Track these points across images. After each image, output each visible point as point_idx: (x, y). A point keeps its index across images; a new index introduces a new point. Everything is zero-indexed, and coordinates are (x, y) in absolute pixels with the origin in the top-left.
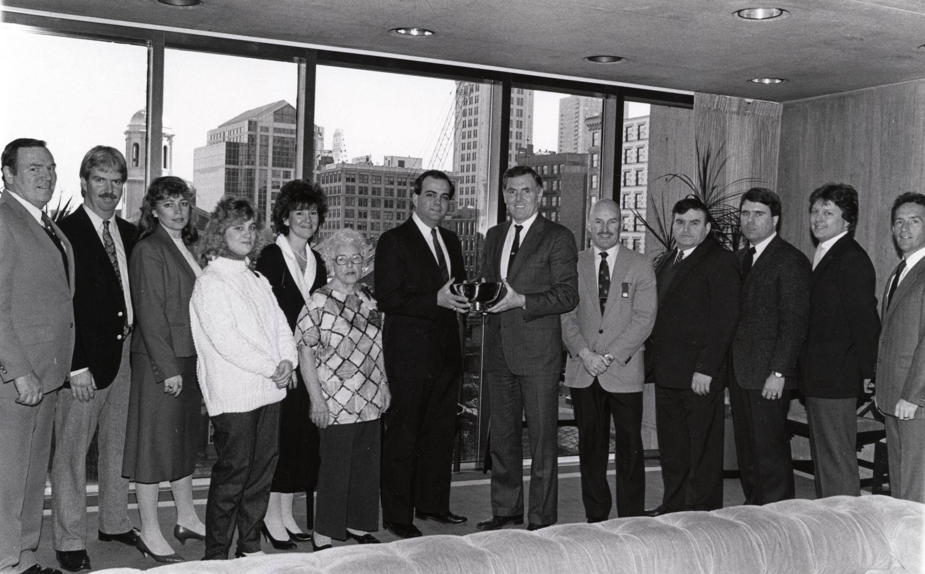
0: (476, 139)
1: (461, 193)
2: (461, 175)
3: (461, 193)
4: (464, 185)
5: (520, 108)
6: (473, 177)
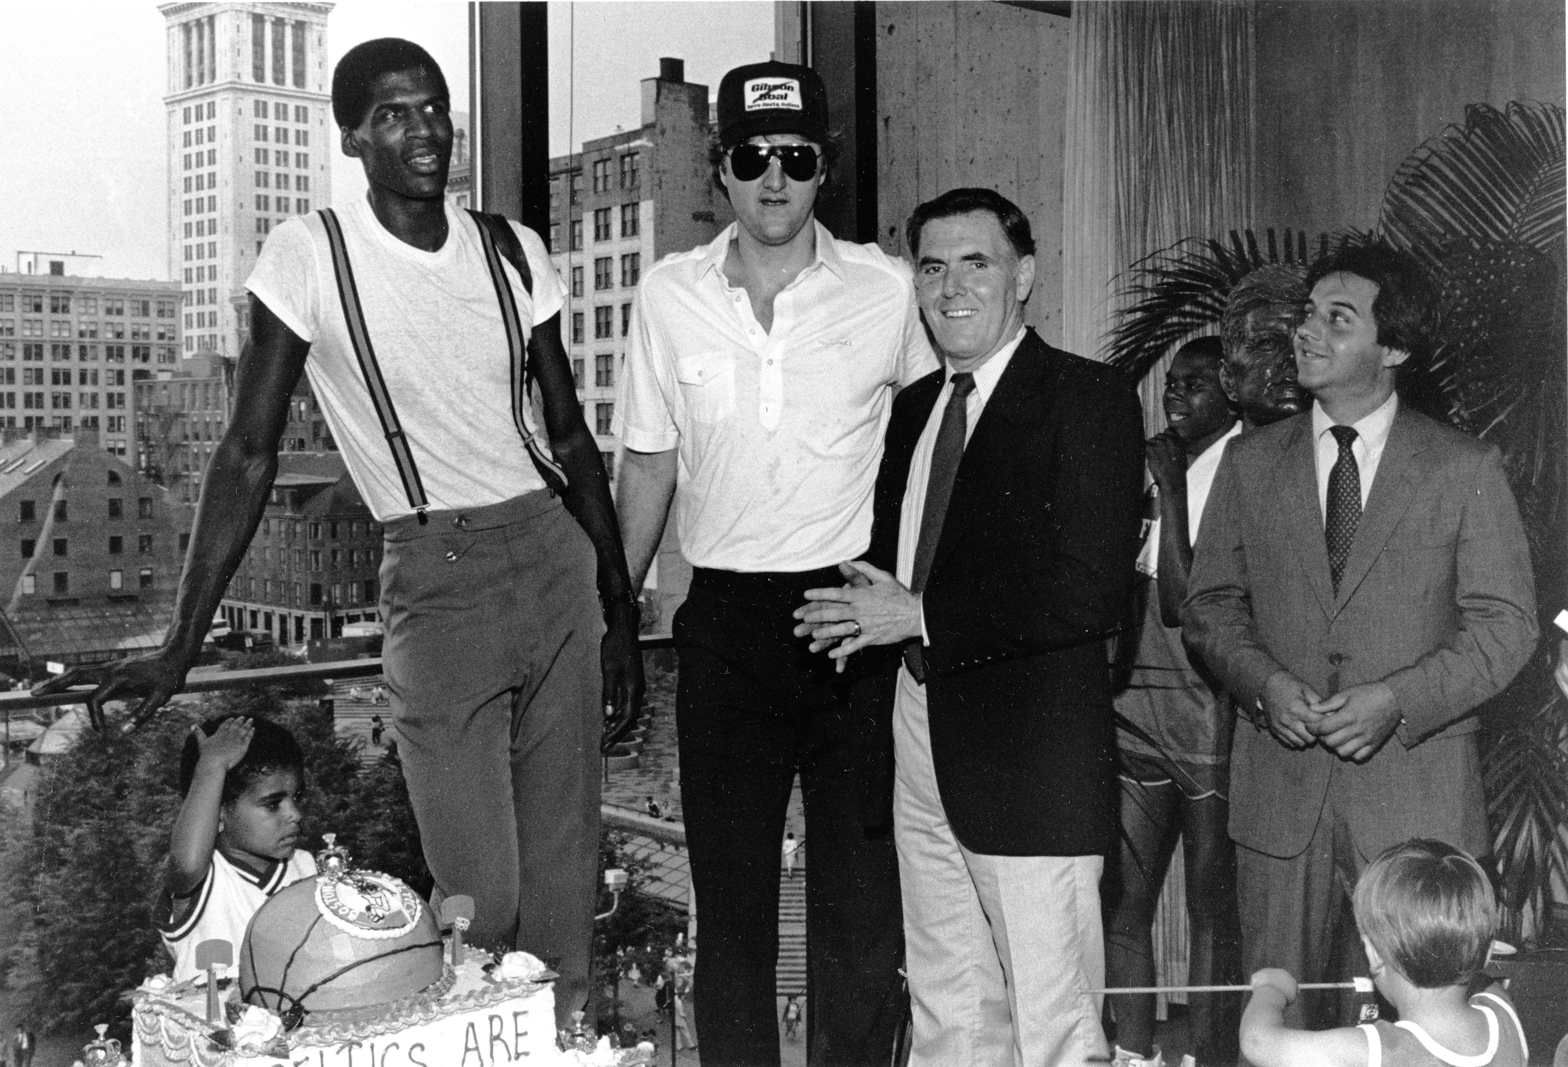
0: (213, 215)
1: (189, 324)
2: (185, 287)
3: (189, 324)
4: (194, 310)
5: (302, 149)
6: (213, 291)
